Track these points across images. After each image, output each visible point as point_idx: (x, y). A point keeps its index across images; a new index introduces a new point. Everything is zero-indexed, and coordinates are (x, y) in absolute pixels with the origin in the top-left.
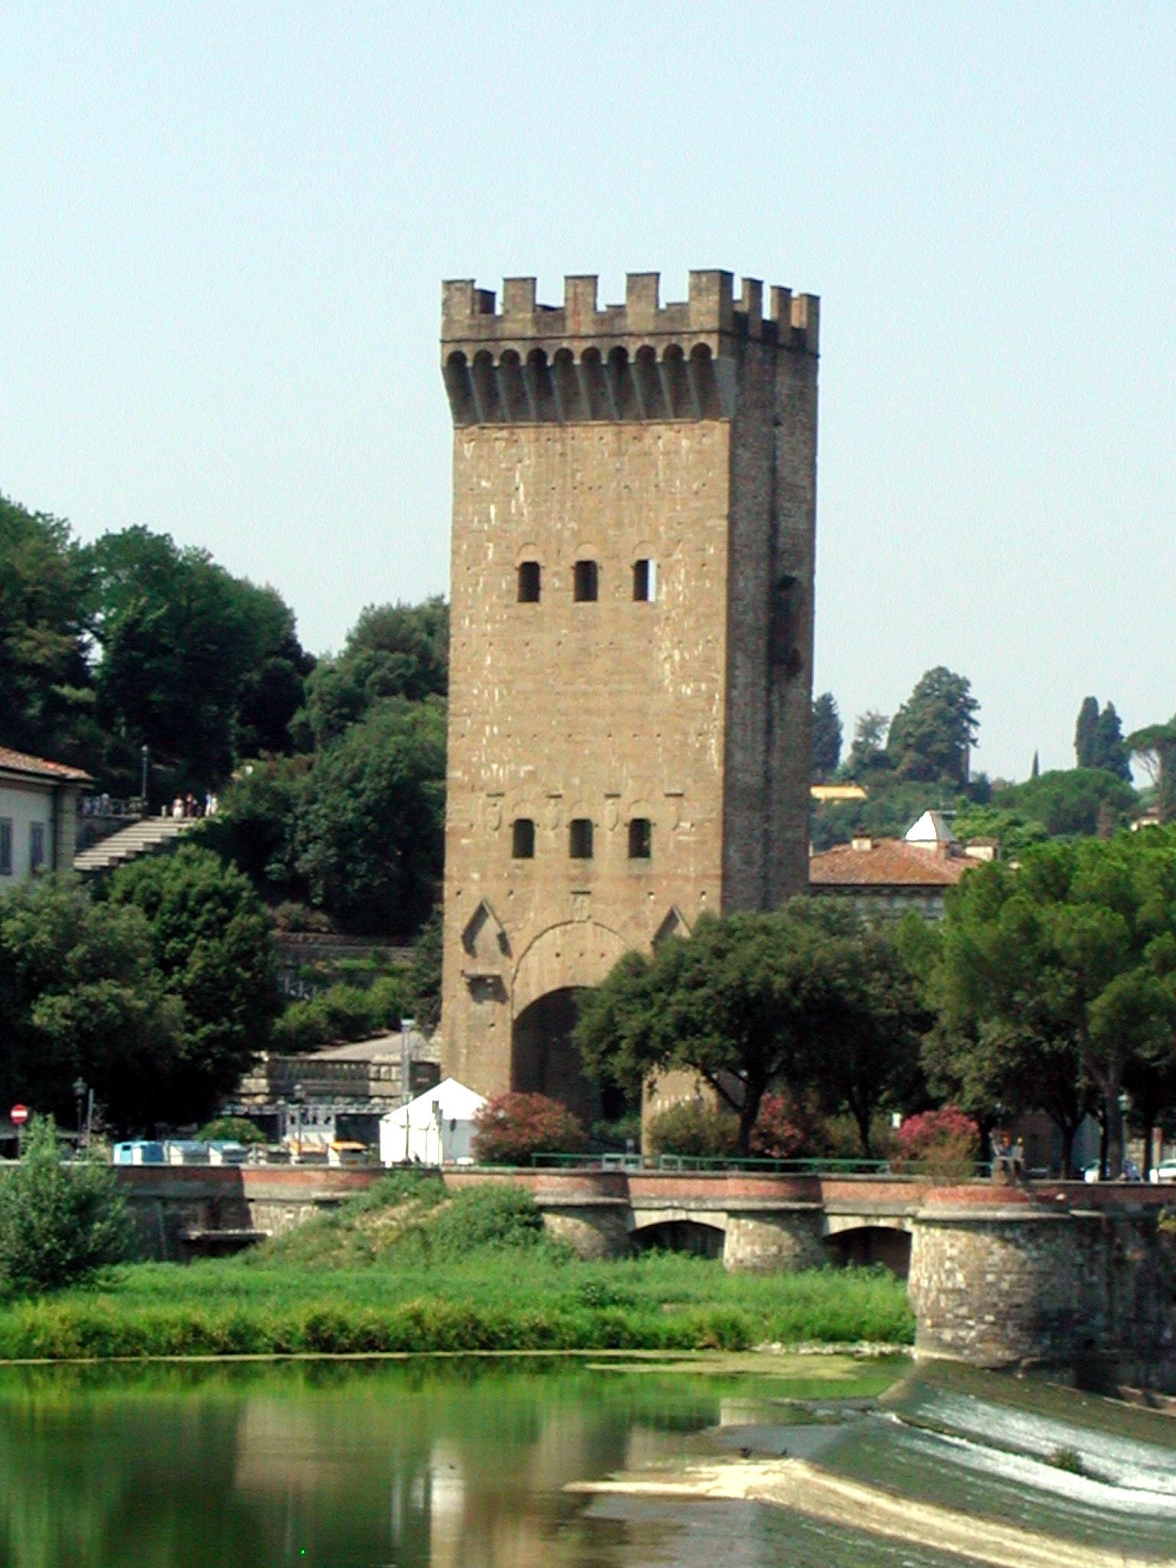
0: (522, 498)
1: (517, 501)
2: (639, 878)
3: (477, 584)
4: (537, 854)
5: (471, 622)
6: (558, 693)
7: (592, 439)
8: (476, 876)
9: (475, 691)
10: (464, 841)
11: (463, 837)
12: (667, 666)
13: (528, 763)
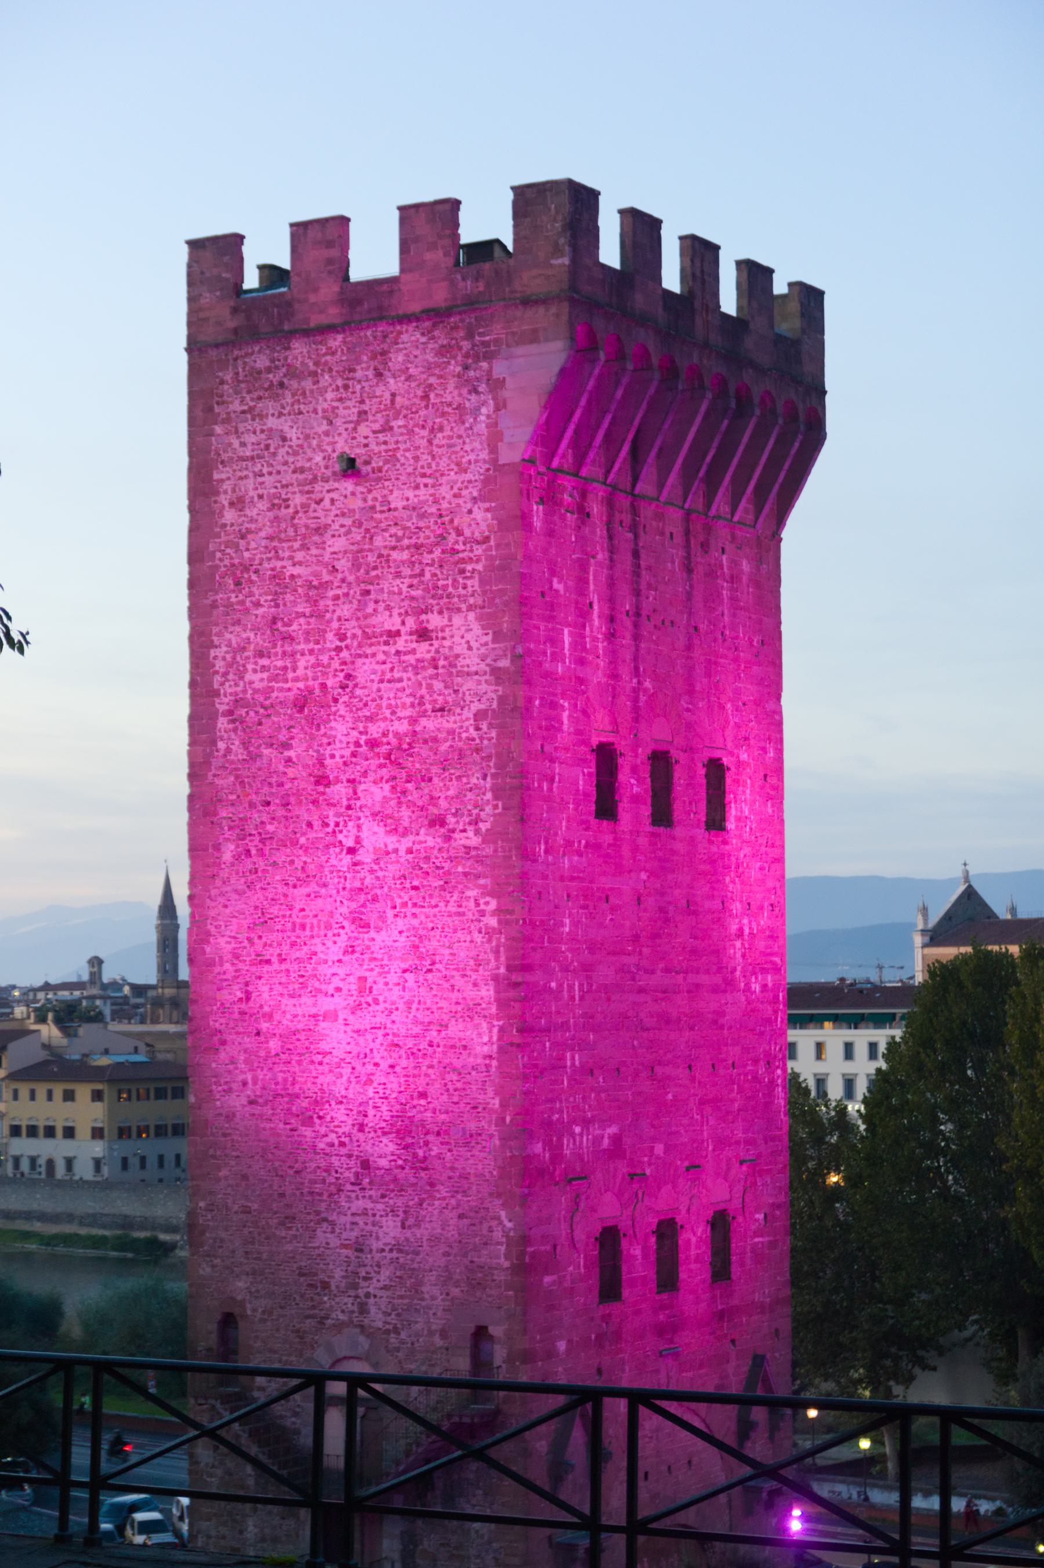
0: (596, 623)
1: (591, 627)
2: (721, 1315)
3: (552, 780)
4: (626, 1293)
5: (546, 852)
6: (641, 990)
7: (662, 534)
8: (562, 1346)
9: (553, 985)
10: (547, 1279)
11: (547, 1272)
12: (738, 944)
13: (612, 1121)
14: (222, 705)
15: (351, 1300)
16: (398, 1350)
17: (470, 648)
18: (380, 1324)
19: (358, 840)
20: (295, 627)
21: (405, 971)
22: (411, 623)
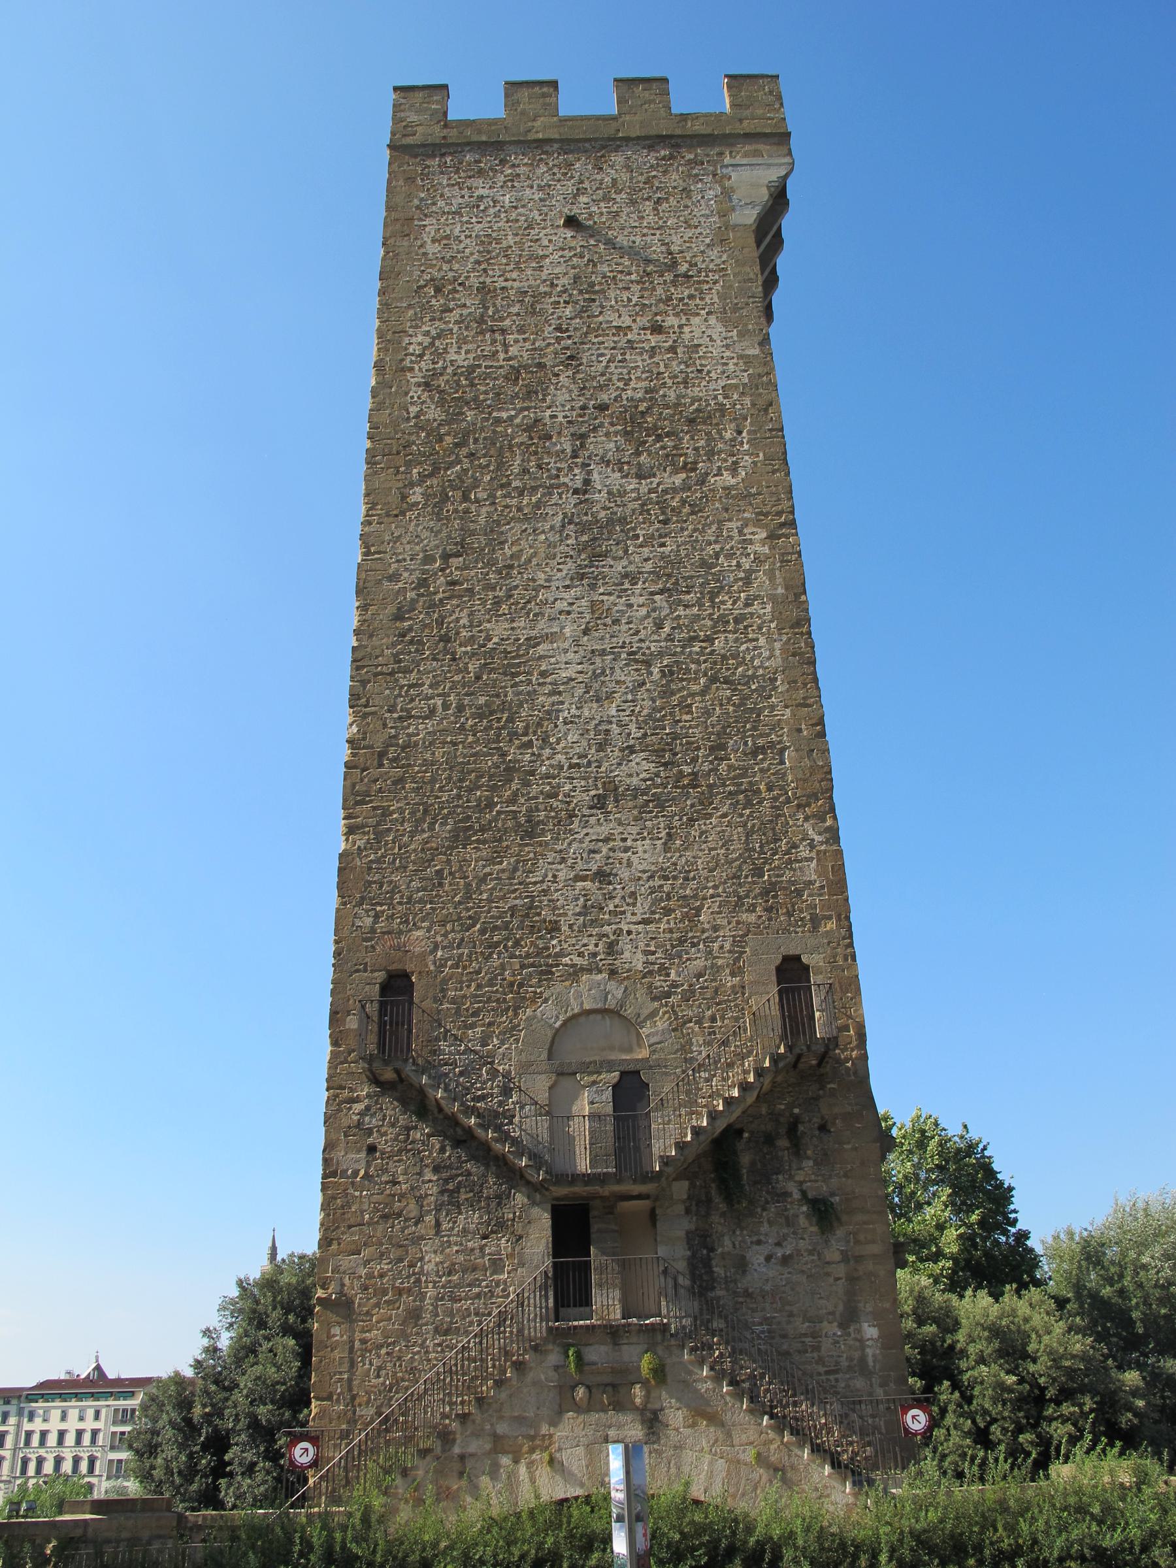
14: (415, 378)
15: (593, 941)
16: (668, 995)
17: (712, 340)
18: (640, 967)
19: (587, 482)
20: (507, 322)
21: (652, 594)
22: (643, 321)
